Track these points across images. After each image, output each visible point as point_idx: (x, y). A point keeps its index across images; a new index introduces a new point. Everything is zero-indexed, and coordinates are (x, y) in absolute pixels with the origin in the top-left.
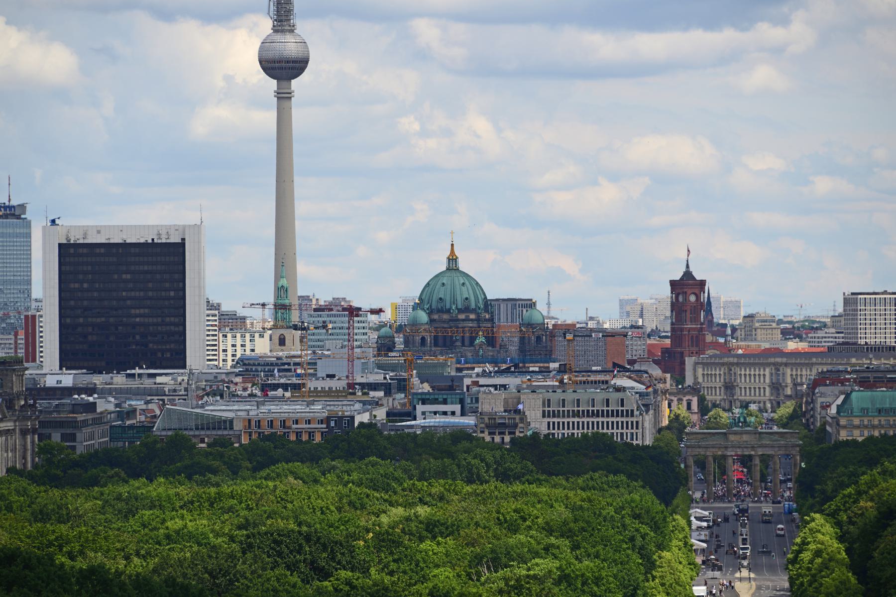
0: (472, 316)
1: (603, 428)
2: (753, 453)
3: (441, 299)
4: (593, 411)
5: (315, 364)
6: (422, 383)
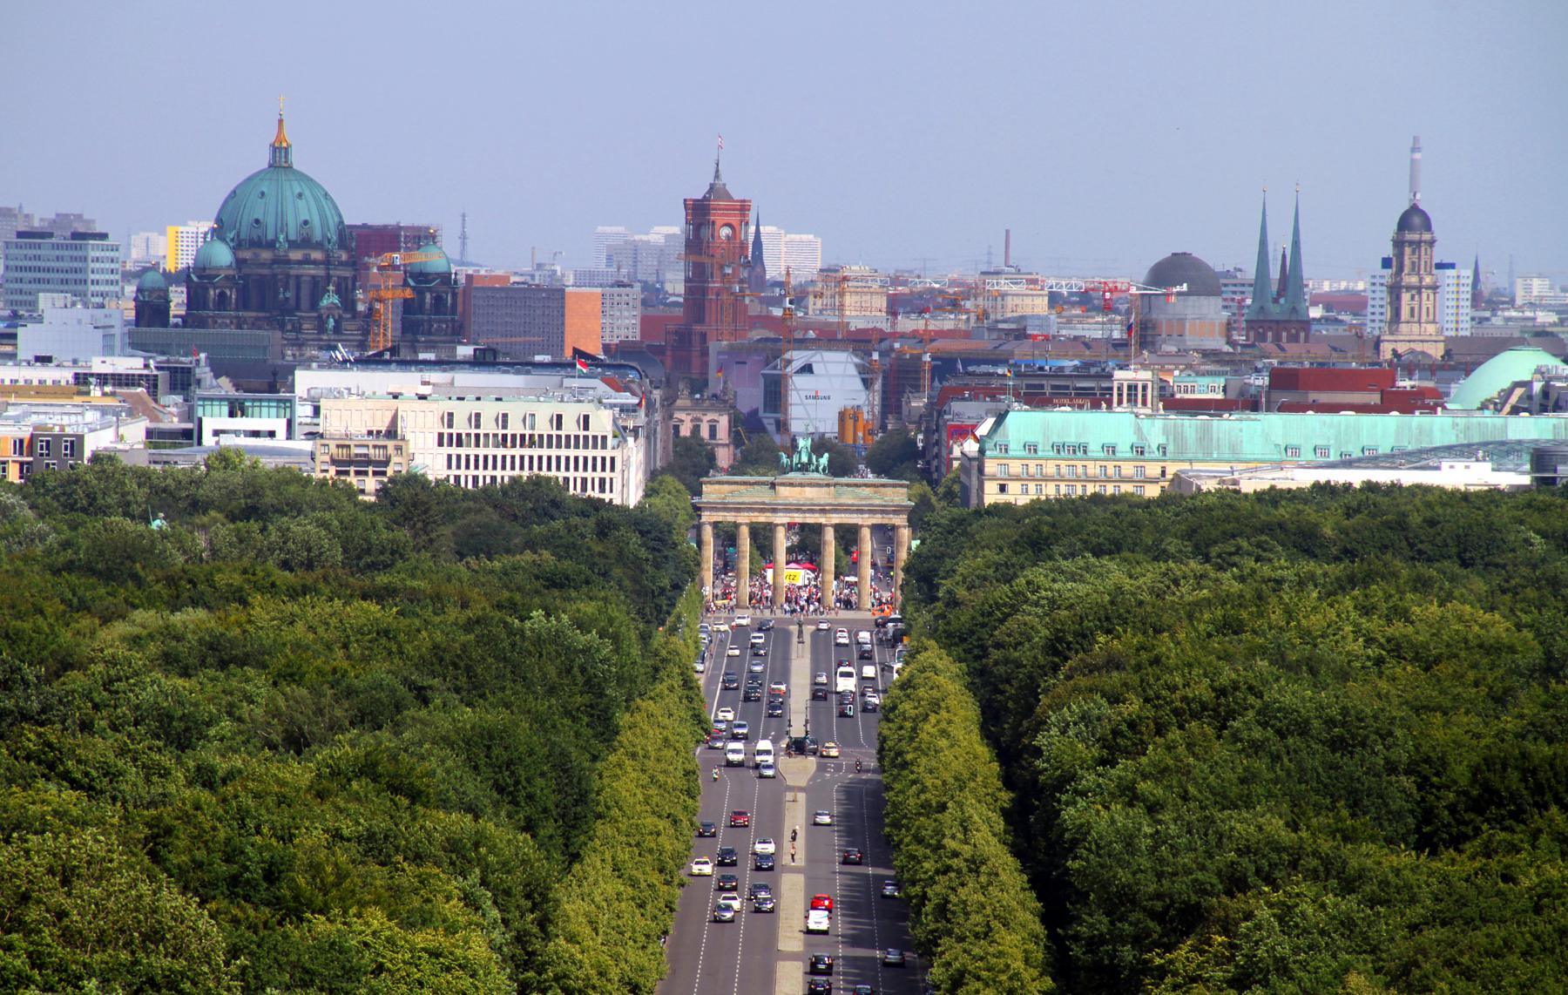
0: (317, 255)
1: (549, 469)
2: (823, 520)
3: (257, 221)
4: (531, 436)
5: (14, 336)
6: (217, 376)
